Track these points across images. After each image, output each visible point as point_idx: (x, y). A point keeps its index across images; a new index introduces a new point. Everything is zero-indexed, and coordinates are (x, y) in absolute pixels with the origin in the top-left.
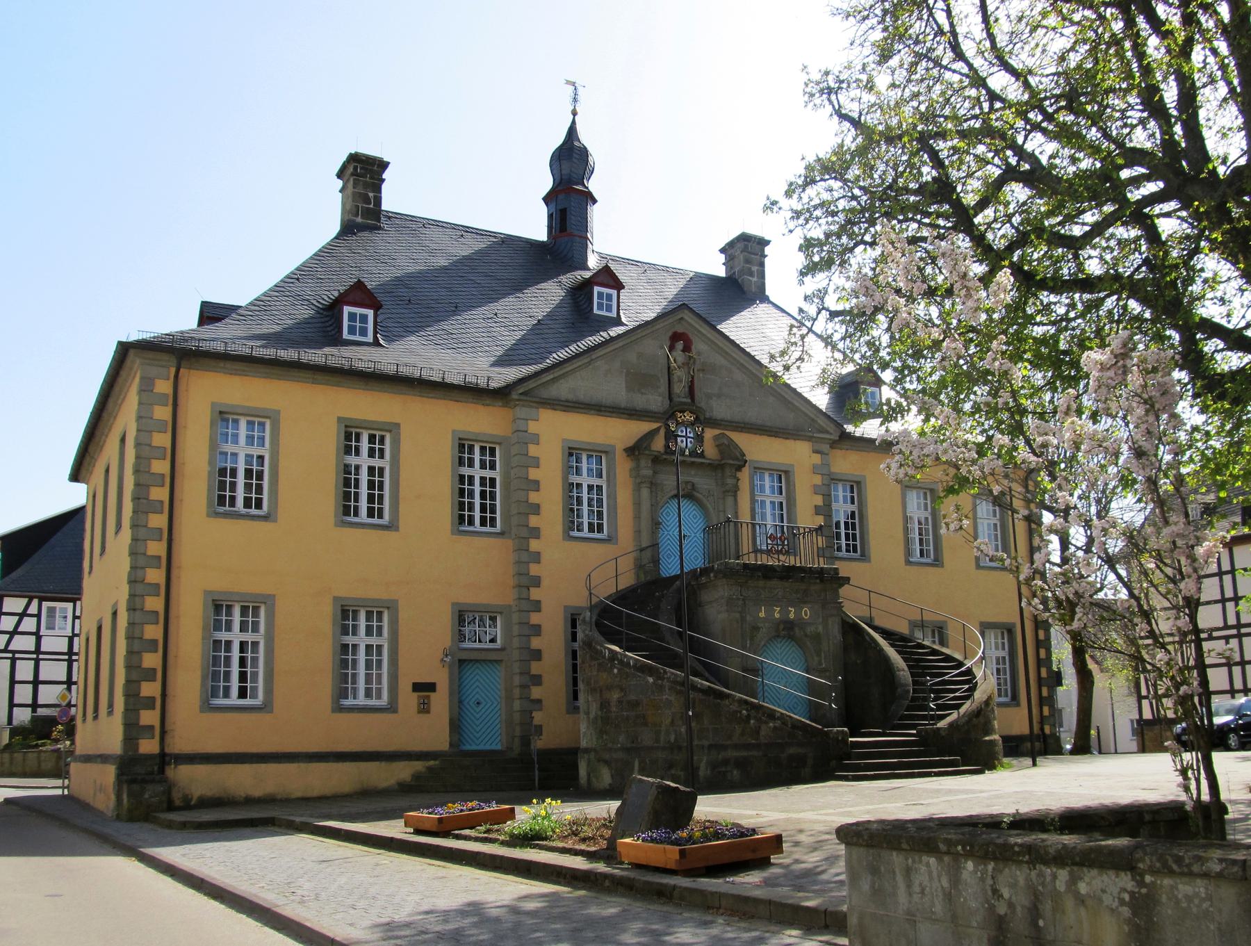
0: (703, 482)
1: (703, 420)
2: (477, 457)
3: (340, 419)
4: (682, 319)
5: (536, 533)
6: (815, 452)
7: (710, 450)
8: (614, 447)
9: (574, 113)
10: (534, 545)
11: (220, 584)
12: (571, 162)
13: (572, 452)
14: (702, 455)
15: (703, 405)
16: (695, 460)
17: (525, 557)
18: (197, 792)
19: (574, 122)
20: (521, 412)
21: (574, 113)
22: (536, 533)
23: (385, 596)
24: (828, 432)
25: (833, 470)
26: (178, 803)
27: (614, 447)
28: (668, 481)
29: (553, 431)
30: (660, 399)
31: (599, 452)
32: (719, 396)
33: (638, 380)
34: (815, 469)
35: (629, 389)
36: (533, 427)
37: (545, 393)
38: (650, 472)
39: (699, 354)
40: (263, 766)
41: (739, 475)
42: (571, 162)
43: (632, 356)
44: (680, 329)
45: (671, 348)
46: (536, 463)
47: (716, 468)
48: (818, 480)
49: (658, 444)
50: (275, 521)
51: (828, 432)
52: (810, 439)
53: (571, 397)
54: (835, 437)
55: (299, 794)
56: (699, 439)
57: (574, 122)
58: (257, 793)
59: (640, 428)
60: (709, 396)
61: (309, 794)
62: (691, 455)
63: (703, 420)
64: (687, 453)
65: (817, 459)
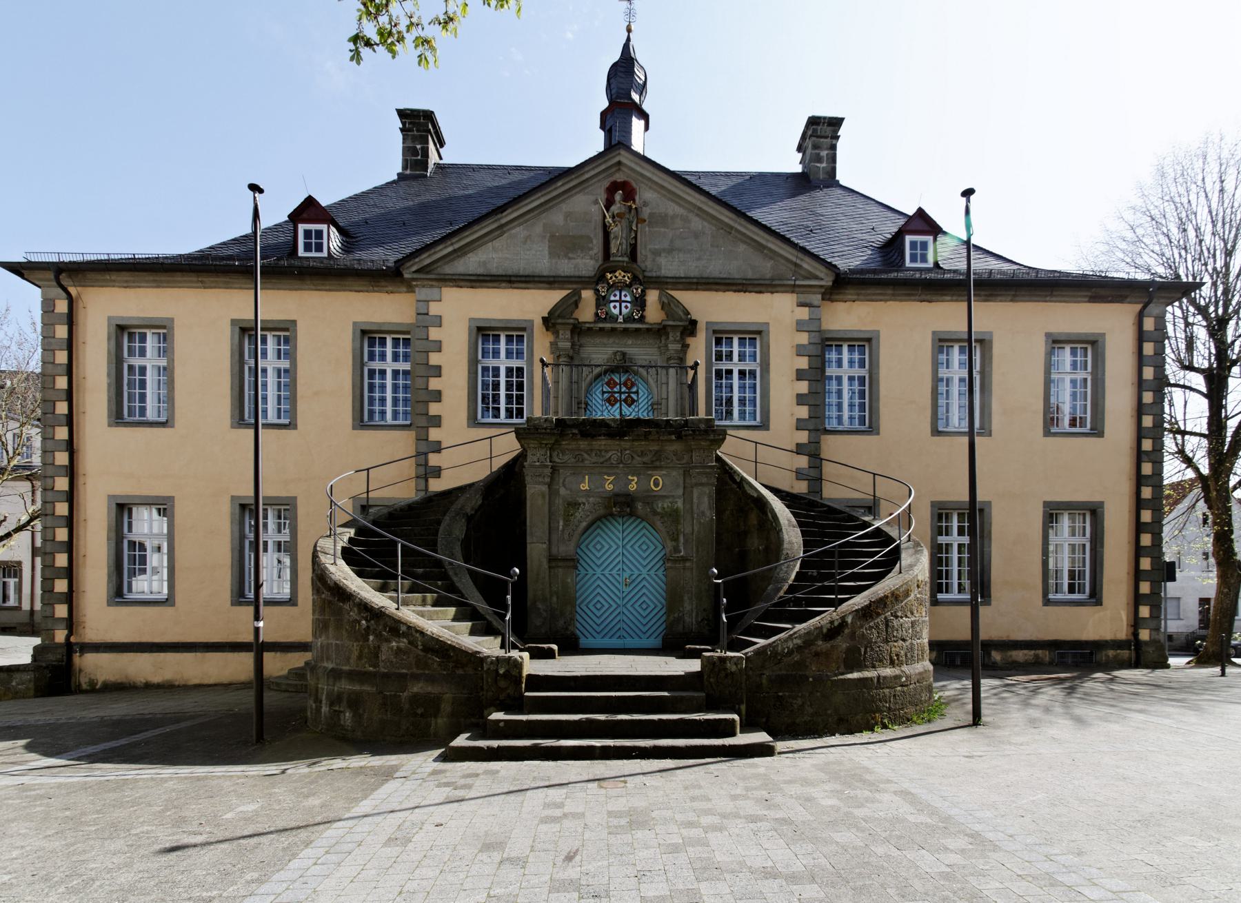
0: (642, 352)
1: (643, 281)
2: (389, 349)
3: (234, 322)
4: (619, 163)
5: (437, 421)
6: (801, 305)
7: (654, 313)
8: (532, 322)
9: (629, 30)
10: (434, 434)
11: (125, 489)
12: (624, 80)
13: (484, 333)
14: (642, 319)
15: (649, 264)
16: (636, 329)
17: (426, 448)
18: (102, 677)
19: (628, 39)
20: (422, 293)
21: (629, 30)
22: (437, 421)
23: (284, 494)
24: (817, 278)
25: (825, 327)
26: (84, 686)
27: (532, 322)
28: (599, 353)
29: (458, 310)
30: (592, 262)
31: (517, 333)
32: (670, 251)
33: (565, 244)
34: (800, 326)
35: (552, 254)
36: (434, 309)
37: (448, 269)
38: (568, 344)
39: (645, 204)
40: (162, 654)
41: (690, 340)
42: (624, 80)
43: (557, 217)
44: (619, 177)
45: (609, 203)
46: (438, 347)
47: (659, 332)
48: (804, 339)
49: (586, 312)
50: (173, 426)
51: (817, 278)
52: (793, 289)
53: (480, 271)
54: (828, 281)
55: (197, 681)
56: (640, 303)
57: (628, 39)
58: (156, 679)
59: (548, 299)
60: (657, 253)
61: (206, 682)
62: (625, 321)
63: (643, 281)
64: (621, 319)
65: (804, 313)
